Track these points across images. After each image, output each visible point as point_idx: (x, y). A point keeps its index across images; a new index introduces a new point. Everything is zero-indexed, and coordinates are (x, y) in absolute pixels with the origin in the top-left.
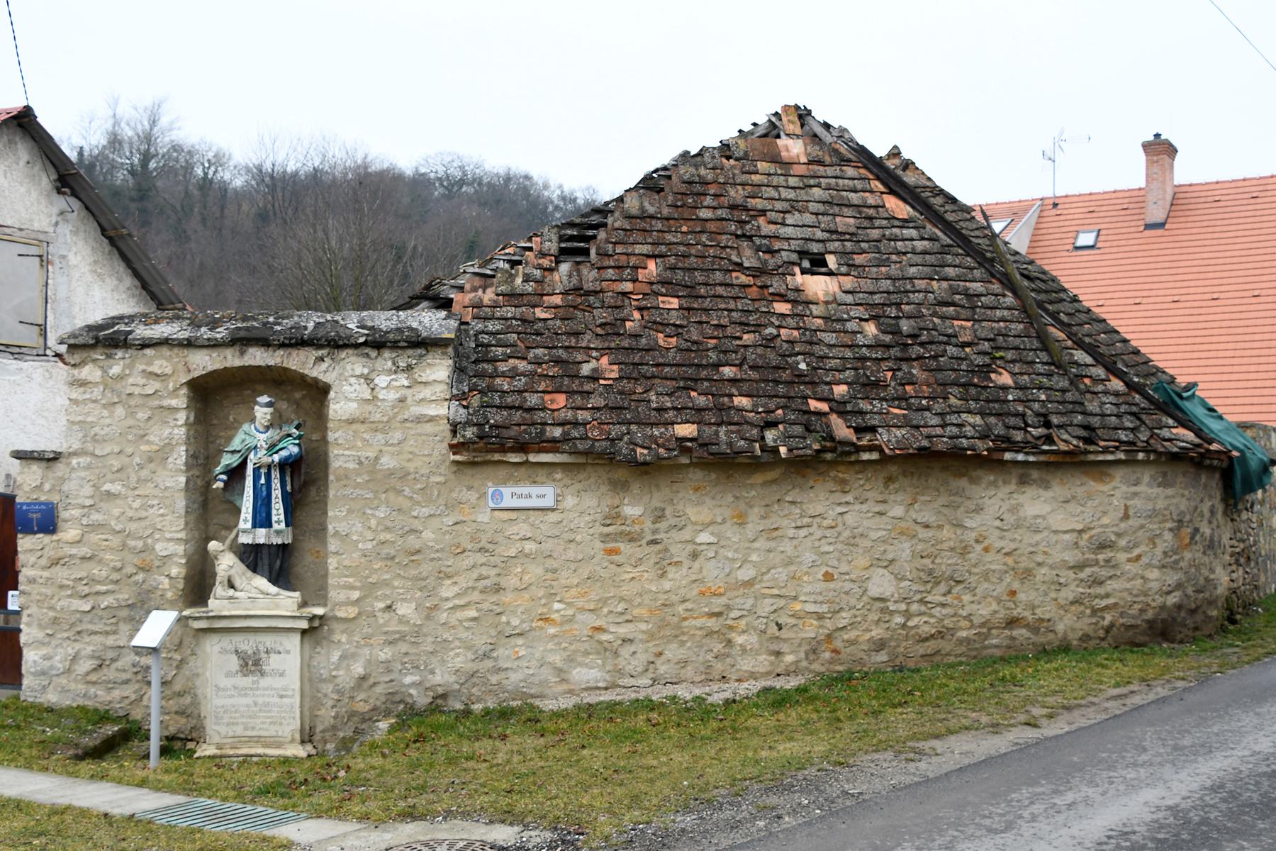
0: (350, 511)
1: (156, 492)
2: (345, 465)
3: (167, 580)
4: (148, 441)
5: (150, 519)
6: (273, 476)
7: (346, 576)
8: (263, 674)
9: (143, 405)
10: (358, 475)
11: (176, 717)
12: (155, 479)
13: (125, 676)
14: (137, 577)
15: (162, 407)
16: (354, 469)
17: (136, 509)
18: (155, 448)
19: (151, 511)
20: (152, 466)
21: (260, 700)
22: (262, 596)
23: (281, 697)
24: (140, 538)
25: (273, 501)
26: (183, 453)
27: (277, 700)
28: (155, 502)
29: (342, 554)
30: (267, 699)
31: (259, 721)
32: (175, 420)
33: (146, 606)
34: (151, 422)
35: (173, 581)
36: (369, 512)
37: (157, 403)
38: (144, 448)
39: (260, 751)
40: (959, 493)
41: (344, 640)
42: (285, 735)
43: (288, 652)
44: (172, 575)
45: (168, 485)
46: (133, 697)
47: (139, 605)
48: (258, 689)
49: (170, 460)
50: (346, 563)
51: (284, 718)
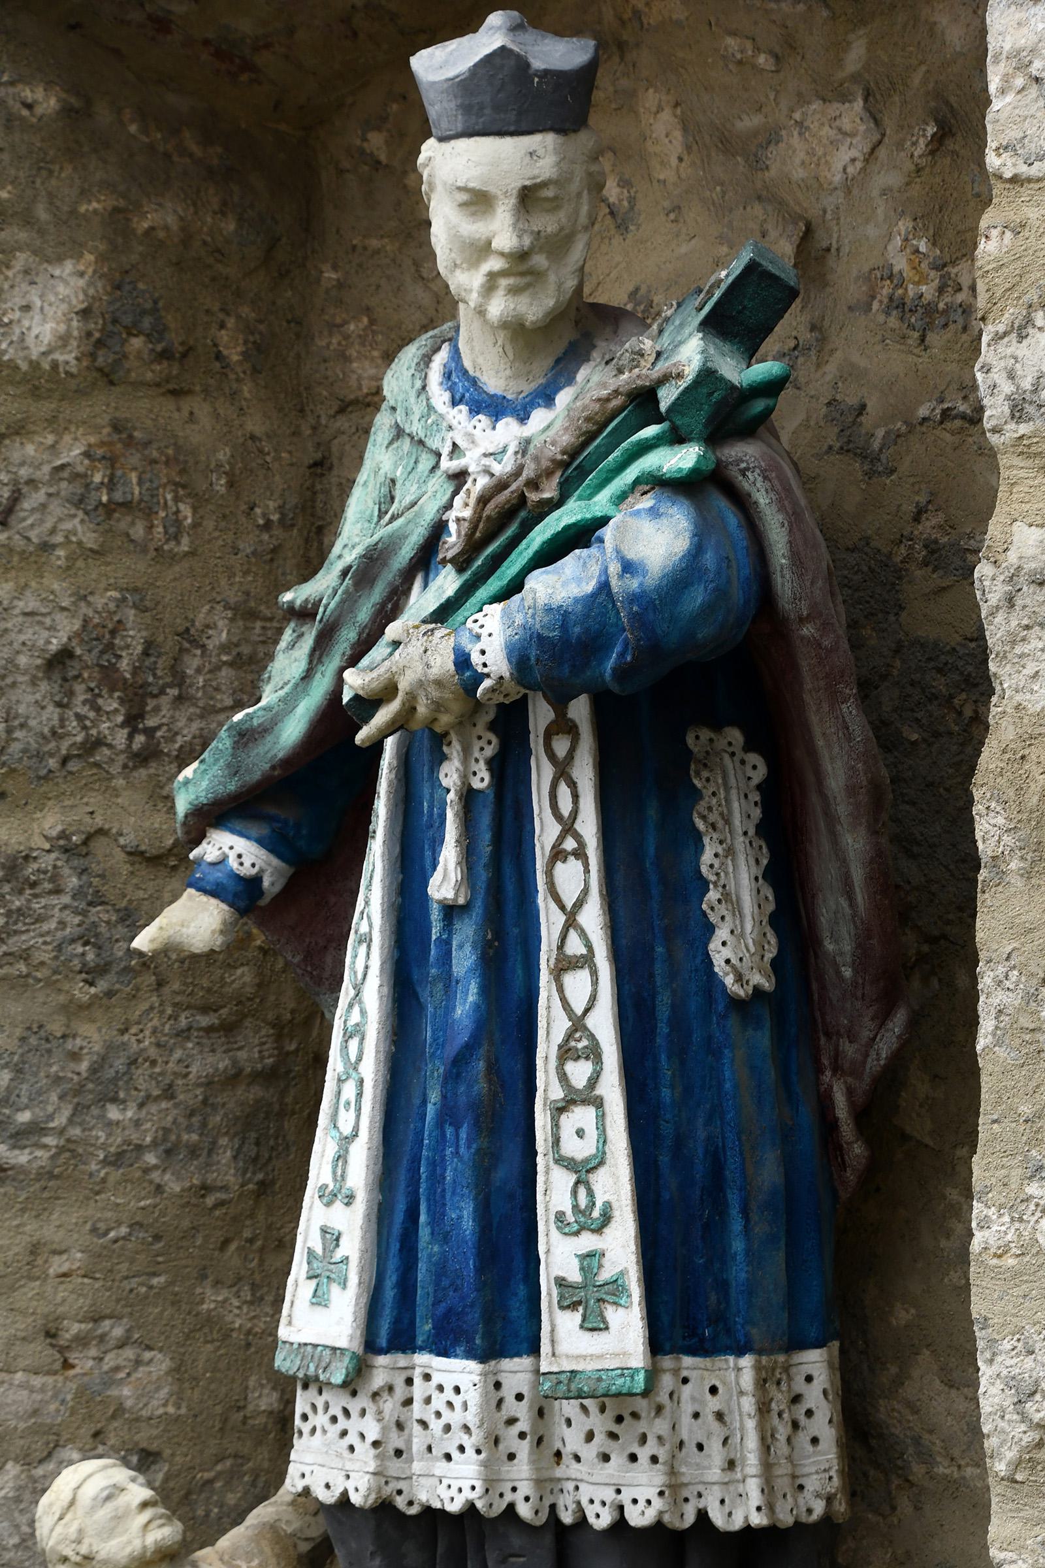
6: (546, 832)
25: (548, 1088)
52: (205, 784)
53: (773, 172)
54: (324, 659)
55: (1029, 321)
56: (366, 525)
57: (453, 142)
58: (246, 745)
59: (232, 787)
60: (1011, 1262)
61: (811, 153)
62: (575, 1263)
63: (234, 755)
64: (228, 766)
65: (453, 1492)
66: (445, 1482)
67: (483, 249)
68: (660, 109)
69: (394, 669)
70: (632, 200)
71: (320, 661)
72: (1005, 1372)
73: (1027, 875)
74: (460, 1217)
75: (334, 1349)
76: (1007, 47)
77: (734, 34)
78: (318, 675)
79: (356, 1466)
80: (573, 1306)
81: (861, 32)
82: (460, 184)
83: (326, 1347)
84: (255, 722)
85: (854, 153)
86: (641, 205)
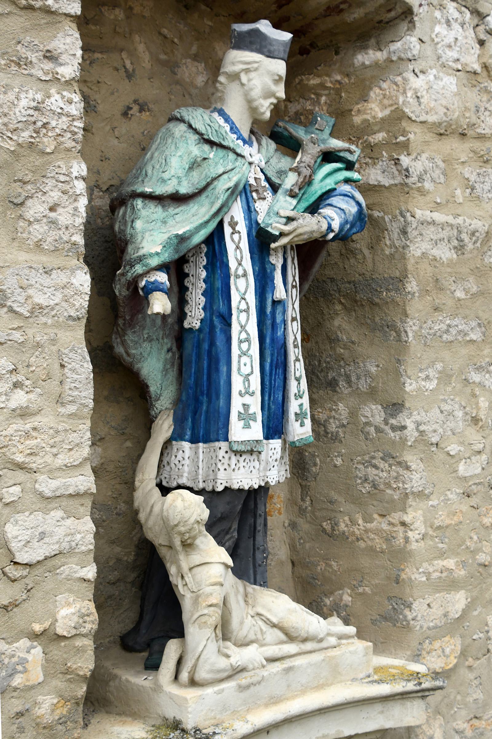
2: (436, 252)
7: (442, 555)
10: (459, 279)
16: (451, 264)
22: (291, 648)
26: (80, 186)
36: (476, 377)
40: (173, 365)
44: (60, 631)
45: (40, 299)
50: (442, 518)
52: (167, 255)
53: (179, 76)
54: (216, 217)
55: (417, 158)
56: (183, 170)
57: (276, 60)
58: (182, 243)
59: (176, 257)
60: (415, 393)
61: (190, 74)
62: (298, 407)
63: (177, 246)
64: (175, 249)
65: (272, 479)
66: (269, 477)
67: (273, 95)
68: (141, 42)
69: (299, 226)
70: (134, 70)
71: (214, 218)
72: (414, 420)
73: (419, 297)
74: (278, 397)
75: (257, 441)
76: (414, 87)
77: (166, 28)
78: (211, 222)
79: (255, 476)
80: (297, 421)
81: (196, 42)
82: (279, 73)
83: (253, 441)
84: (187, 235)
85: (203, 79)
86: (137, 72)
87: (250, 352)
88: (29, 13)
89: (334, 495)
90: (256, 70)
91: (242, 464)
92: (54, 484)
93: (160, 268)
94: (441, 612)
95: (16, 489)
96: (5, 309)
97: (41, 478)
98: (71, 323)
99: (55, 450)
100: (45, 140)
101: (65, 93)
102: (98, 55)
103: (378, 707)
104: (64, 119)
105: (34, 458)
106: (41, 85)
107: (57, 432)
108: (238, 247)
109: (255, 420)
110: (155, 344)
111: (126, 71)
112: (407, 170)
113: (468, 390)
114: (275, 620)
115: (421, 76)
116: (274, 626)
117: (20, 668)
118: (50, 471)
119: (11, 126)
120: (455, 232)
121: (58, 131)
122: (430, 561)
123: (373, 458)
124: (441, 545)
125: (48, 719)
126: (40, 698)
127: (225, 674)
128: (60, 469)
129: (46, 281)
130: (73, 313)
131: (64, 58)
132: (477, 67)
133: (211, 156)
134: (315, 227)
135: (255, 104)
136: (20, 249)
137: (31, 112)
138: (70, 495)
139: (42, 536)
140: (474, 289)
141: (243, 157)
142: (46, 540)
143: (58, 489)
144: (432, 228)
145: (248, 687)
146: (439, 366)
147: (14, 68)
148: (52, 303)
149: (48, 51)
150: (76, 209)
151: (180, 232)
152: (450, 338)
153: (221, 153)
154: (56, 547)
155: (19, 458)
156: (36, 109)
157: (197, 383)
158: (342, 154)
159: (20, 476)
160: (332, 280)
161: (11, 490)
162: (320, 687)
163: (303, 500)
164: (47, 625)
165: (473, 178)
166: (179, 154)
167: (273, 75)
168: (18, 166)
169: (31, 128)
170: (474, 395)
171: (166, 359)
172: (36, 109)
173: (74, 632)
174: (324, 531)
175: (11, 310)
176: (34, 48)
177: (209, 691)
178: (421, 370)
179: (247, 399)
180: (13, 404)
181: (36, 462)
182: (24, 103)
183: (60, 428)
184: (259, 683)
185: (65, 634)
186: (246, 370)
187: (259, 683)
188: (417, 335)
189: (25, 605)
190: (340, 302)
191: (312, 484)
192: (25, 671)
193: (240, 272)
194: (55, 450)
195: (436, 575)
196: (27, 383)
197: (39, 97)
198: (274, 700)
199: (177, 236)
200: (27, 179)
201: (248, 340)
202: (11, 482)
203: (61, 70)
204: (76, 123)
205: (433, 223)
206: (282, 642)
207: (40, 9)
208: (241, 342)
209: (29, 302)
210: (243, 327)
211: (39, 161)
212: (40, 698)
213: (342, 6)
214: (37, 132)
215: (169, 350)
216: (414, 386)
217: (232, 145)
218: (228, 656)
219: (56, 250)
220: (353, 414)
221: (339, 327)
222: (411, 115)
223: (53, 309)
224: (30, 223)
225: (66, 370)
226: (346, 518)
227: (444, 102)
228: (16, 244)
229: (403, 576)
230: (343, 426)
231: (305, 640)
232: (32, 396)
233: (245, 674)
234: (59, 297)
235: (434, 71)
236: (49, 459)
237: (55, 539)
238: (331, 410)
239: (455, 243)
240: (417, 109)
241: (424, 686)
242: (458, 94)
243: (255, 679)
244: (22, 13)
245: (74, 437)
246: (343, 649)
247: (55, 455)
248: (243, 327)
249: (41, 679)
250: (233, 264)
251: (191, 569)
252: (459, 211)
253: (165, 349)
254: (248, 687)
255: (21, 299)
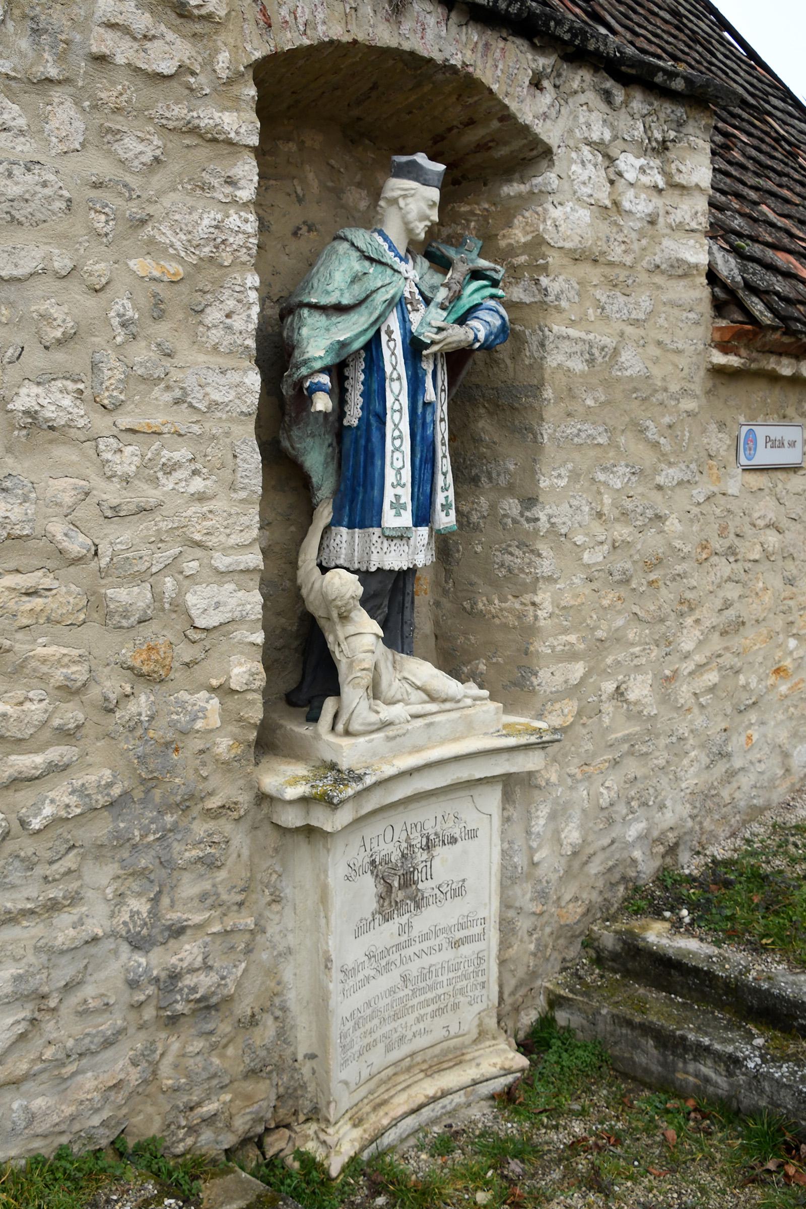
0: (575, 476)
1: (182, 419)
2: (570, 364)
3: (215, 703)
4: (152, 241)
5: (166, 510)
7: (566, 631)
8: (418, 902)
9: (141, 113)
10: (590, 388)
11: (249, 1086)
12: (175, 375)
13: (107, 1024)
14: (132, 708)
15: (194, 131)
16: (583, 375)
17: (126, 480)
18: (175, 268)
19: (168, 483)
20: (162, 330)
21: (414, 968)
22: (432, 707)
23: (457, 944)
24: (139, 577)
26: (253, 296)
27: (448, 955)
28: (182, 454)
29: (556, 581)
30: (426, 961)
31: (411, 1018)
32: (230, 182)
33: (157, 794)
34: (158, 180)
35: (232, 703)
36: (601, 477)
37: (179, 111)
38: (141, 265)
39: (430, 1087)
41: (554, 778)
42: (465, 1028)
43: (472, 834)
44: (234, 686)
45: (216, 396)
46: (134, 1076)
47: (138, 794)
48: (409, 943)
49: (214, 315)
50: (567, 599)
51: (462, 991)
53: (343, 201)
59: (338, 361)
67: (427, 218)
87: (403, 448)
88: (214, 146)
89: (474, 578)
90: (412, 196)
91: (393, 548)
92: (227, 560)
93: (323, 370)
94: (562, 679)
95: (195, 564)
96: (186, 405)
97: (216, 555)
98: (243, 418)
99: (228, 531)
100: (224, 254)
101: (242, 214)
102: (272, 182)
103: (505, 756)
104: (241, 236)
105: (210, 537)
106: (221, 207)
107: (230, 515)
108: (393, 353)
109: (405, 509)
110: (317, 440)
111: (297, 196)
112: (546, 290)
113: (594, 488)
114: (419, 683)
115: (559, 207)
116: (418, 688)
117: (200, 714)
118: (224, 549)
119: (194, 243)
120: (587, 347)
121: (235, 247)
122: (555, 636)
123: (510, 546)
124: (565, 623)
125: (226, 757)
126: (218, 740)
127: (376, 727)
128: (232, 547)
129: (222, 380)
130: (245, 410)
131: (242, 183)
132: (608, 203)
133: (371, 271)
134: (463, 337)
135: (412, 225)
136: (199, 351)
137: (212, 230)
138: (242, 571)
139: (217, 605)
140: (603, 399)
141: (399, 272)
142: (221, 609)
143: (230, 565)
144: (567, 343)
145: (394, 738)
146: (570, 466)
147: (199, 192)
148: (226, 400)
149: (229, 177)
150: (249, 316)
151: (342, 339)
152: (580, 441)
153: (380, 268)
154: (229, 615)
155: (197, 537)
156: (216, 227)
157: (354, 476)
158: (488, 273)
159: (199, 553)
160: (478, 386)
161: (191, 564)
162: (456, 739)
163: (446, 582)
164: (222, 680)
165: (603, 299)
166: (342, 268)
167: (428, 200)
168: (200, 277)
169: (212, 244)
170: (599, 493)
171: (327, 454)
172: (216, 227)
173: (245, 687)
174: (464, 609)
175: (191, 406)
176: (217, 175)
177: (361, 740)
178: (554, 469)
179: (399, 491)
180: (192, 489)
181: (212, 541)
182: (206, 222)
183: (233, 511)
184: (404, 735)
185: (238, 688)
186: (398, 464)
187: (404, 735)
188: (552, 438)
189: (204, 663)
190: (484, 406)
191: (455, 568)
192: (205, 717)
193: (395, 376)
194: (228, 531)
195: (559, 648)
196: (204, 471)
197: (219, 217)
198: (417, 749)
199: (339, 342)
200: (206, 289)
201: (400, 437)
202: (191, 558)
203: (239, 193)
204: (251, 240)
205: (568, 337)
206: (425, 702)
207: (223, 141)
208: (394, 439)
209: (207, 398)
210: (396, 426)
211: (218, 273)
212: (218, 740)
213: (491, 144)
214: (217, 247)
215: (329, 446)
216: (548, 483)
217: (389, 262)
218: (378, 712)
219: (231, 352)
220: (493, 507)
221: (483, 429)
222: (550, 241)
223: (227, 405)
224: (209, 328)
225: (238, 460)
226: (484, 599)
227: (579, 232)
228: (196, 347)
229: (532, 649)
230: (484, 517)
231: (445, 701)
232: (208, 482)
233: (392, 727)
234: (232, 395)
235: (571, 204)
236: (223, 538)
237: (229, 608)
238: (473, 503)
239: (587, 356)
240: (556, 236)
241: (544, 739)
242: (591, 225)
243: (401, 732)
244: (208, 145)
245: (244, 520)
246: (478, 708)
247: (228, 535)
248: (396, 426)
249: (219, 724)
250: (388, 369)
251: (346, 638)
252: (591, 328)
253: (327, 443)
254: (394, 738)
255: (200, 396)
